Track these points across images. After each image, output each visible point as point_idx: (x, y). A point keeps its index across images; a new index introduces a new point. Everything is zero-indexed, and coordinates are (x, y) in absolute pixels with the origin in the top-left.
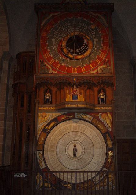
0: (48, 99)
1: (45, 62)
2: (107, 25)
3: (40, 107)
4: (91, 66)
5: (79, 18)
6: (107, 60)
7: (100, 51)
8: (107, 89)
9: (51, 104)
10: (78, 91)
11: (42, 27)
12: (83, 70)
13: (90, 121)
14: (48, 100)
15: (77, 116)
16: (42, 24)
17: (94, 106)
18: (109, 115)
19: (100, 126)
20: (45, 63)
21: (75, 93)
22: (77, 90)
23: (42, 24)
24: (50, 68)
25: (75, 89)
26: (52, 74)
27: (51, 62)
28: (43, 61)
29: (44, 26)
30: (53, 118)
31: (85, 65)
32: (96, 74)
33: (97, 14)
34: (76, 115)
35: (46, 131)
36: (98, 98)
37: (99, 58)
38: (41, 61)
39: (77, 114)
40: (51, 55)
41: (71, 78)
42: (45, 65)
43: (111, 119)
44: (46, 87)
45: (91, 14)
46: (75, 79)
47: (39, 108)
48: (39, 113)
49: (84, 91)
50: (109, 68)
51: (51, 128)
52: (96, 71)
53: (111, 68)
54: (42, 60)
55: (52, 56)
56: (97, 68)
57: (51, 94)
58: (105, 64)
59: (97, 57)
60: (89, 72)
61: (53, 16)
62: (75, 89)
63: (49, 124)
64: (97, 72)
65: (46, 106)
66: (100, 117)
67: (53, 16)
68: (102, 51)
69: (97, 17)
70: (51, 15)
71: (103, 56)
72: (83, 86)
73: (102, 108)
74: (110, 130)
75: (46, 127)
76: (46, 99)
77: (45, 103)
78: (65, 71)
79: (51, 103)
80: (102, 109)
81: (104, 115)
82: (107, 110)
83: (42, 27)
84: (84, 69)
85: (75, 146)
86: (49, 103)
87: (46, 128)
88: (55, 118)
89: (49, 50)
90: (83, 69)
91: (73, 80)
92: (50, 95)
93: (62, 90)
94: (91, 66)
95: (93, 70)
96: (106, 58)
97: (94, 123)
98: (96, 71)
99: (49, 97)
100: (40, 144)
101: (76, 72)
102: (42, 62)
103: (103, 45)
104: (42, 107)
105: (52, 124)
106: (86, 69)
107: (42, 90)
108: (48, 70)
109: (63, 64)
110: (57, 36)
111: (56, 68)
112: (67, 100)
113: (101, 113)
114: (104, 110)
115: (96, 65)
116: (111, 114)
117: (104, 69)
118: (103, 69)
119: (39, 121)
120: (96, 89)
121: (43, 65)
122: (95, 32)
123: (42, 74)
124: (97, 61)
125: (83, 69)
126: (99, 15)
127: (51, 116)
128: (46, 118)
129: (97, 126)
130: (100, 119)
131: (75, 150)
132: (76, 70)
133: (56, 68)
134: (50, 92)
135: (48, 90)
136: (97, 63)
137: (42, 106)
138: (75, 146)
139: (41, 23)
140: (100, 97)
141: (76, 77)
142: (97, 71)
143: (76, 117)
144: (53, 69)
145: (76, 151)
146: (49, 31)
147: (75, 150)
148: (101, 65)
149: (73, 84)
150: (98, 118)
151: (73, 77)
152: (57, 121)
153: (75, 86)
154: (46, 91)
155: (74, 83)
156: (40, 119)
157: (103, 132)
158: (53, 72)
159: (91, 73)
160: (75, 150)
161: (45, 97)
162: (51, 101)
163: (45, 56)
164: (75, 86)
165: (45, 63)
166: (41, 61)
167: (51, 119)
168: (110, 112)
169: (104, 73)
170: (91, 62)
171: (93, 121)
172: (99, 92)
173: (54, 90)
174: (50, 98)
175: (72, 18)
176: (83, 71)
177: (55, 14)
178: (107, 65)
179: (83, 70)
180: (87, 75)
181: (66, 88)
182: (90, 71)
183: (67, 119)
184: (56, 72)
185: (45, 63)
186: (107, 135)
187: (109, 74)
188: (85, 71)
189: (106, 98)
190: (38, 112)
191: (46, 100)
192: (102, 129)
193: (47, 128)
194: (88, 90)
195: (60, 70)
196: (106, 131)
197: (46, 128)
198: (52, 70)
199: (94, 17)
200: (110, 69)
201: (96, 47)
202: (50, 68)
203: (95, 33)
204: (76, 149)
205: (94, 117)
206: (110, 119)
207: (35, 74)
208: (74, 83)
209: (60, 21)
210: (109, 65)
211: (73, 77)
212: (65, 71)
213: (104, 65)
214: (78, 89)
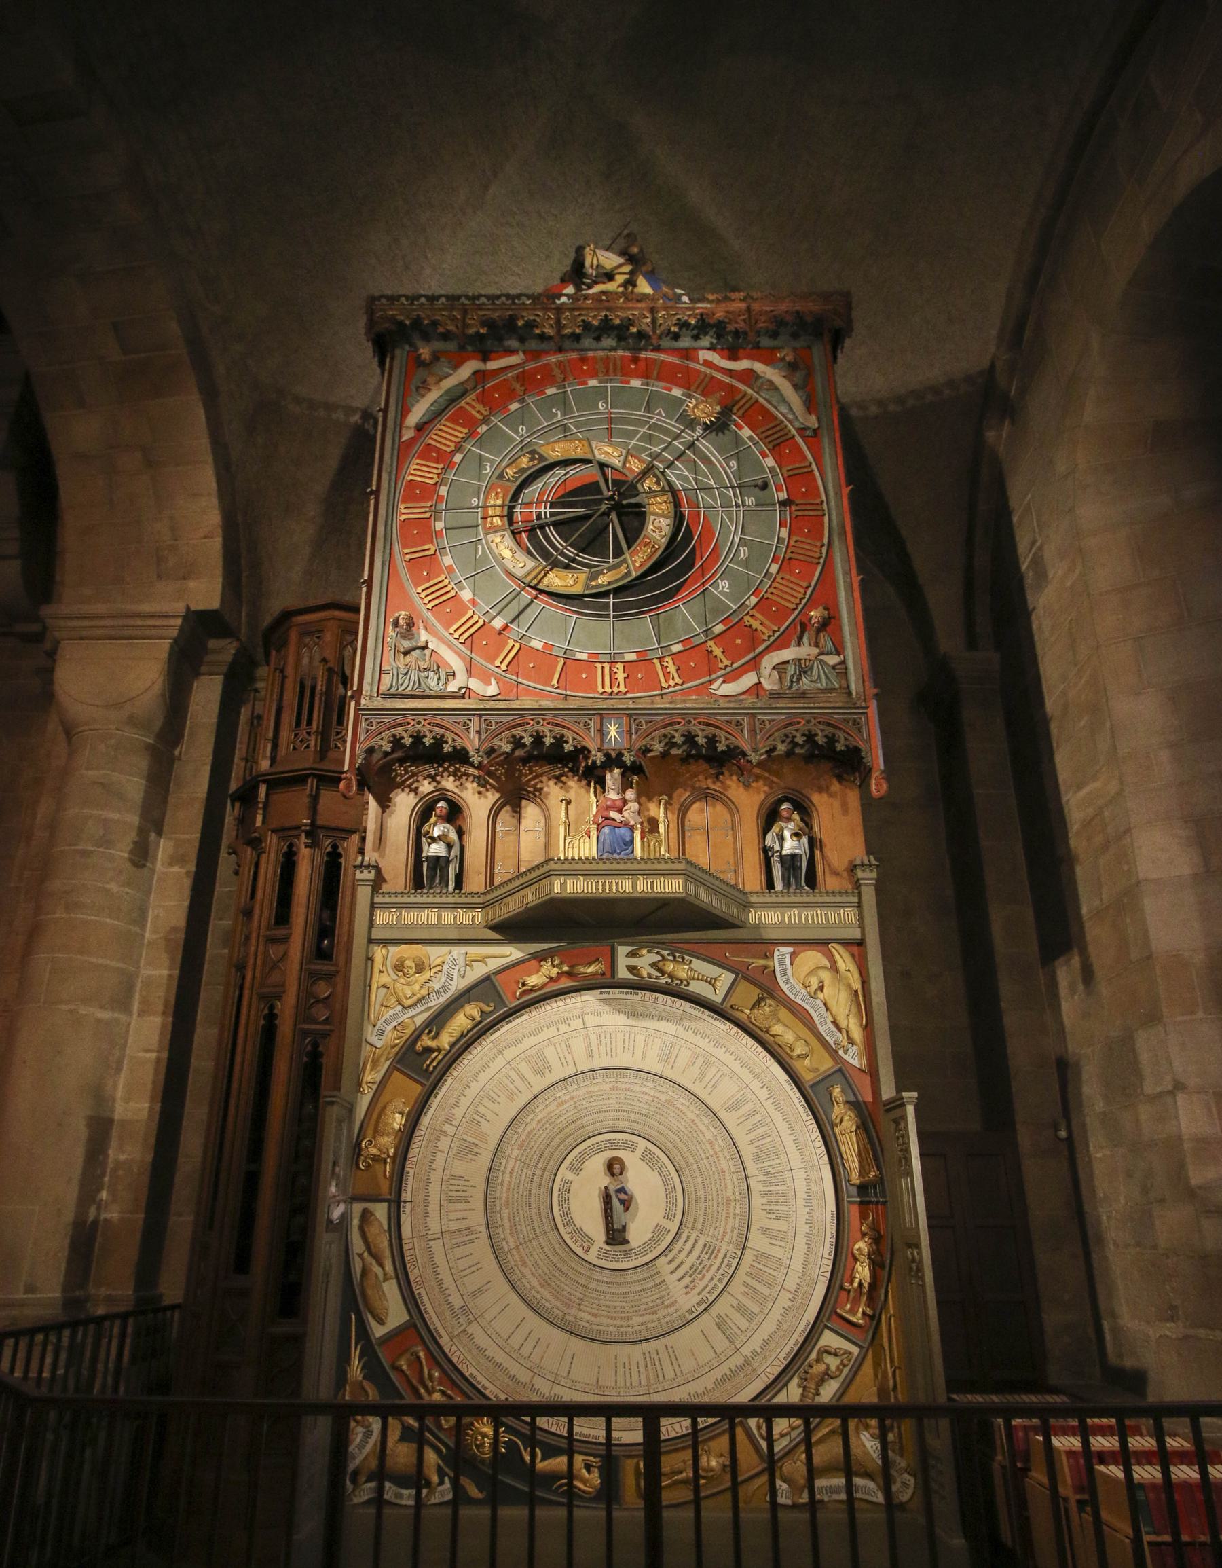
0: (438, 858)
1: (426, 628)
3: (385, 907)
4: (717, 651)
5: (636, 383)
6: (815, 614)
7: (774, 568)
8: (818, 799)
9: (455, 889)
11: (408, 435)
12: (667, 674)
13: (718, 999)
15: (632, 969)
16: (413, 418)
17: (747, 906)
18: (845, 962)
19: (785, 1032)
20: (424, 636)
21: (613, 814)
22: (625, 802)
23: (413, 418)
24: (456, 664)
25: (613, 795)
26: (463, 697)
28: (411, 624)
29: (420, 428)
31: (677, 648)
32: (749, 700)
33: (743, 364)
34: (623, 962)
38: (396, 624)
39: (632, 954)
40: (462, 588)
41: (586, 724)
42: (425, 647)
43: (857, 986)
44: (426, 787)
45: (707, 363)
46: (613, 731)
48: (379, 952)
50: (833, 660)
51: (452, 1045)
52: (749, 680)
53: (843, 662)
54: (402, 614)
55: (466, 595)
56: (754, 665)
57: (460, 833)
58: (805, 640)
59: (753, 600)
60: (703, 689)
62: (613, 795)
65: (425, 899)
66: (784, 974)
67: (476, 373)
68: (786, 564)
73: (793, 915)
74: (856, 1063)
75: (418, 1037)
76: (428, 857)
78: (547, 682)
80: (795, 919)
81: (812, 958)
82: (828, 926)
83: (408, 435)
84: (672, 669)
85: (614, 1167)
86: (447, 886)
87: (419, 1046)
88: (487, 979)
89: (447, 560)
90: (664, 668)
91: (602, 732)
92: (453, 836)
93: (530, 811)
94: (717, 651)
95: (729, 678)
97: (738, 1015)
98: (749, 680)
99: (450, 846)
100: (373, 1151)
101: (622, 689)
103: (789, 535)
104: (400, 907)
107: (404, 803)
108: (442, 673)
109: (537, 644)
111: (492, 661)
113: (790, 949)
114: (807, 927)
116: (853, 956)
117: (803, 668)
118: (791, 669)
119: (377, 996)
121: (407, 644)
122: (737, 456)
124: (756, 624)
125: (664, 668)
126: (758, 367)
128: (426, 975)
129: (767, 1032)
130: (784, 987)
131: (615, 1202)
132: (621, 676)
133: (492, 661)
135: (441, 804)
136: (753, 638)
137: (406, 899)
138: (614, 1167)
139: (405, 411)
140: (777, 847)
142: (756, 681)
143: (623, 973)
145: (622, 1202)
146: (453, 453)
149: (599, 758)
150: (768, 988)
151: (603, 716)
153: (613, 778)
155: (607, 755)
156: (384, 986)
157: (808, 1077)
158: (474, 684)
159: (719, 692)
161: (418, 849)
164: (613, 778)
165: (423, 632)
166: (396, 624)
167: (458, 985)
168: (845, 943)
169: (803, 695)
170: (719, 628)
171: (733, 1000)
174: (455, 851)
175: (593, 383)
176: (664, 684)
178: (817, 645)
179: (667, 674)
180: (693, 701)
181: (553, 791)
182: (711, 682)
183: (566, 983)
184: (492, 690)
185: (423, 632)
186: (837, 1091)
188: (678, 680)
189: (818, 854)
190: (370, 941)
191: (425, 865)
192: (798, 1051)
195: (517, 674)
196: (827, 1064)
197: (419, 1046)
198: (470, 675)
199: (727, 379)
200: (841, 670)
201: (742, 542)
202: (456, 664)
203: (734, 463)
204: (622, 1190)
205: (740, 973)
206: (849, 986)
207: (358, 695)
208: (607, 755)
209: (522, 401)
210: (830, 646)
212: (547, 682)
213: (799, 645)
214: (630, 794)
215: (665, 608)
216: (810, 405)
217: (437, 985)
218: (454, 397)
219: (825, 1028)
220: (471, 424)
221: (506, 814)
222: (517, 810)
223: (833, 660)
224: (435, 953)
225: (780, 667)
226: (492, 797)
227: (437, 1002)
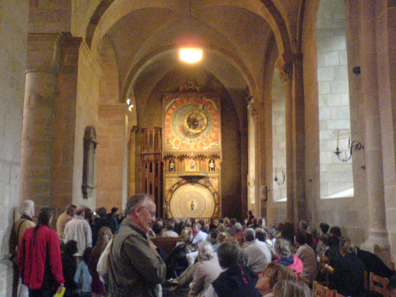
2: (217, 110)
6: (216, 138)
10: (194, 163)
14: (172, 169)
20: (170, 141)
27: (174, 140)
30: (176, 182)
33: (209, 100)
35: (172, 191)
36: (209, 167)
37: (210, 137)
47: (167, 175)
49: (199, 161)
54: (167, 138)
55: (175, 135)
56: (208, 145)
61: (175, 102)
63: (173, 187)
64: (208, 148)
69: (209, 102)
70: (173, 101)
71: (213, 135)
72: (198, 158)
77: (170, 171)
79: (175, 171)
85: (192, 202)
89: (172, 130)
91: (191, 154)
93: (182, 161)
95: (206, 146)
96: (215, 137)
102: (168, 140)
105: (176, 186)
106: (200, 146)
107: (168, 161)
110: (178, 119)
112: (186, 170)
115: (207, 142)
120: (208, 160)
123: (168, 150)
126: (211, 101)
127: (175, 181)
134: (174, 162)
136: (208, 142)
138: (192, 202)
141: (194, 152)
143: (193, 181)
144: (176, 146)
147: (192, 206)
148: (212, 142)
150: (209, 182)
151: (191, 152)
152: (179, 184)
154: (170, 162)
160: (192, 206)
162: (175, 170)
163: (170, 136)
172: (210, 162)
173: (176, 161)
177: (176, 100)
180: (201, 151)
184: (178, 148)
186: (215, 194)
187: (217, 150)
193: (172, 189)
194: (202, 161)
196: (215, 191)
211: (191, 152)
215: (198, 137)
216: (217, 107)
217: (173, 182)
218: (172, 105)
219: (214, 187)
220: (174, 109)
221: (180, 162)
222: (181, 161)
223: (217, 145)
224: (173, 179)
225: (211, 146)
226: (178, 160)
227: (173, 185)
